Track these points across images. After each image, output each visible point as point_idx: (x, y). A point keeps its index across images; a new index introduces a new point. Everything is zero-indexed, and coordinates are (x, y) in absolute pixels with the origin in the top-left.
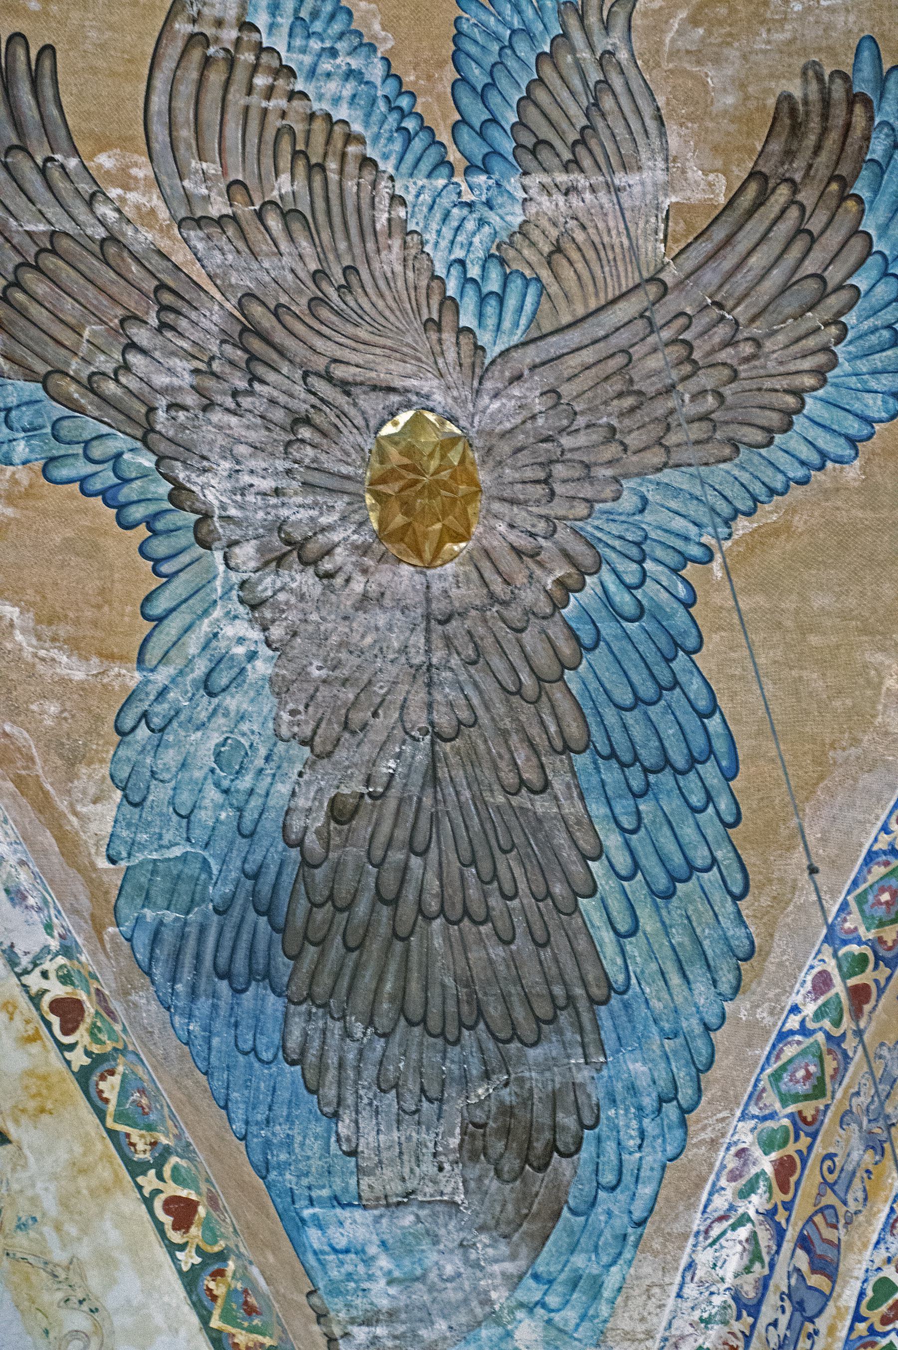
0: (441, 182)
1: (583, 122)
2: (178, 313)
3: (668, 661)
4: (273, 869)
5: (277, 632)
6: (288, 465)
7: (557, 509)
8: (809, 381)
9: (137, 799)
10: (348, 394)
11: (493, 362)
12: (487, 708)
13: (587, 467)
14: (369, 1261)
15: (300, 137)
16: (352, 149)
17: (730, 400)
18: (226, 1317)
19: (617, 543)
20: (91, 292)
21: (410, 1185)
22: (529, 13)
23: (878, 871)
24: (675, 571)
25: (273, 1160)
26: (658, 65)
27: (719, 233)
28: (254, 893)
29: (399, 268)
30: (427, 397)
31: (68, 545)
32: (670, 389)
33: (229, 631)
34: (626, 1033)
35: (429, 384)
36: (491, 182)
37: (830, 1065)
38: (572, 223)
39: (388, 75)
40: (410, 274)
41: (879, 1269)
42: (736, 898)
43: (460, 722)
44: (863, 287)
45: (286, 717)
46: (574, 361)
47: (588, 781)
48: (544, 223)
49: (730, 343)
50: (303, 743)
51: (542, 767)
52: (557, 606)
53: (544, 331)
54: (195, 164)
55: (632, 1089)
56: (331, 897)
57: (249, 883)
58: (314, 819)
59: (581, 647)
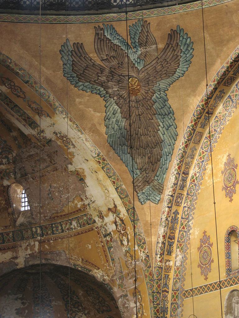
2: (103, 71)
7: (149, 87)
8: (177, 67)
9: (108, 127)
10: (124, 77)
13: (153, 81)
17: (168, 71)
19: (157, 90)
24: (164, 92)
27: (164, 51)
32: (161, 71)
37: (184, 154)
42: (176, 129)
46: (149, 69)
47: (157, 118)
49: (167, 64)
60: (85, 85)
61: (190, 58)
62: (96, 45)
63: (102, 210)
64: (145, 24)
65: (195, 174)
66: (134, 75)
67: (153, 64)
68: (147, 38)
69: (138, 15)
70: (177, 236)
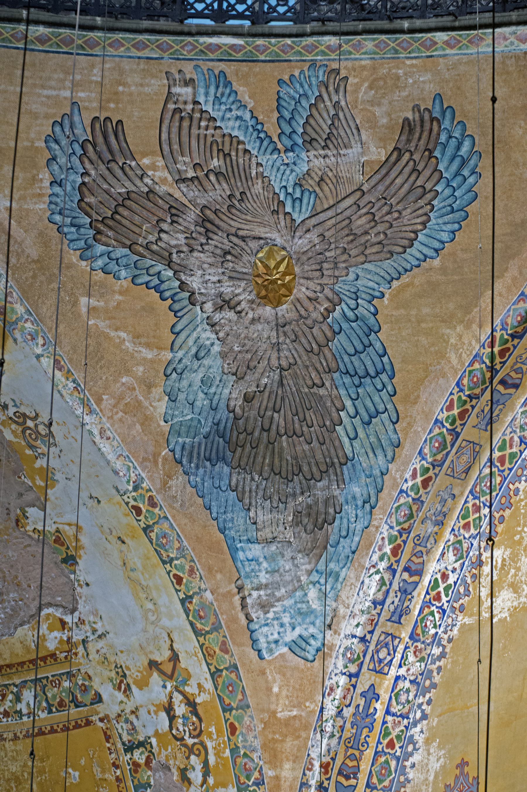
0: (276, 156)
1: (328, 131)
3: (368, 336)
4: (224, 421)
5: (221, 335)
6: (223, 270)
7: (325, 281)
8: (420, 227)
10: (244, 241)
12: (300, 358)
13: (336, 263)
14: (259, 564)
16: (240, 147)
17: (389, 236)
18: (193, 617)
19: (347, 293)
20: (145, 212)
21: (275, 535)
22: (306, 87)
24: (370, 302)
25: (227, 527)
26: (356, 107)
27: (383, 171)
28: (217, 431)
29: (261, 191)
31: (143, 308)
33: (204, 336)
35: (274, 235)
38: (327, 169)
39: (252, 117)
40: (266, 193)
42: (394, 423)
44: (440, 190)
45: (226, 366)
47: (339, 382)
48: (316, 170)
49: (389, 213)
50: (233, 374)
54: (180, 158)
55: (354, 498)
56: (245, 430)
57: (215, 427)
60: (113, 255)
61: (464, 203)
63: (128, 663)
64: (332, 81)
65: (445, 577)
66: (279, 241)
68: (333, 124)
69: (310, 49)
70: (365, 766)
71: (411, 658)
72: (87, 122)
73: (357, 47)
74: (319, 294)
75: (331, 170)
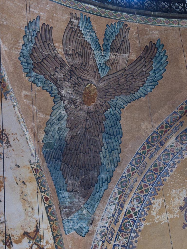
3: (116, 121)
7: (106, 99)
8: (141, 85)
10: (83, 81)
11: (102, 78)
13: (111, 94)
15: (83, 44)
19: (113, 105)
20: (52, 63)
22: (116, 29)
23: (138, 156)
24: (119, 109)
25: (57, 184)
27: (134, 64)
28: (60, 148)
29: (92, 64)
30: (93, 82)
32: (123, 85)
34: (103, 171)
36: (106, 53)
39: (96, 36)
40: (93, 64)
41: (129, 208)
42: (119, 154)
43: (89, 127)
46: (112, 79)
47: (104, 136)
48: (112, 59)
49: (132, 79)
50: (69, 128)
51: (98, 134)
52: (104, 113)
53: (109, 74)
54: (68, 46)
56: (69, 149)
58: (69, 138)
59: (106, 119)
60: (37, 77)
61: (158, 79)
62: (66, 34)
63: (13, 234)
64: (124, 28)
66: (94, 82)
67: (117, 75)
68: (122, 44)
69: (119, 16)
71: (120, 238)
72: (41, 25)
73: (135, 18)
74: (104, 104)
75: (117, 61)
